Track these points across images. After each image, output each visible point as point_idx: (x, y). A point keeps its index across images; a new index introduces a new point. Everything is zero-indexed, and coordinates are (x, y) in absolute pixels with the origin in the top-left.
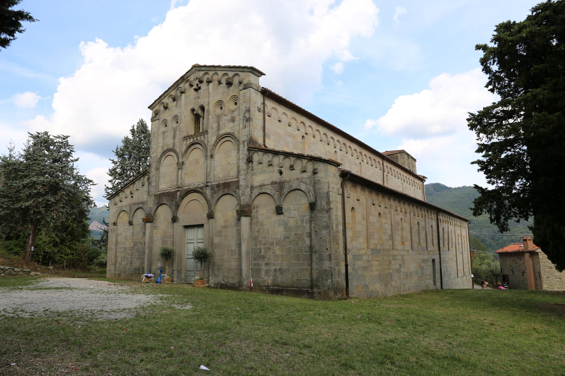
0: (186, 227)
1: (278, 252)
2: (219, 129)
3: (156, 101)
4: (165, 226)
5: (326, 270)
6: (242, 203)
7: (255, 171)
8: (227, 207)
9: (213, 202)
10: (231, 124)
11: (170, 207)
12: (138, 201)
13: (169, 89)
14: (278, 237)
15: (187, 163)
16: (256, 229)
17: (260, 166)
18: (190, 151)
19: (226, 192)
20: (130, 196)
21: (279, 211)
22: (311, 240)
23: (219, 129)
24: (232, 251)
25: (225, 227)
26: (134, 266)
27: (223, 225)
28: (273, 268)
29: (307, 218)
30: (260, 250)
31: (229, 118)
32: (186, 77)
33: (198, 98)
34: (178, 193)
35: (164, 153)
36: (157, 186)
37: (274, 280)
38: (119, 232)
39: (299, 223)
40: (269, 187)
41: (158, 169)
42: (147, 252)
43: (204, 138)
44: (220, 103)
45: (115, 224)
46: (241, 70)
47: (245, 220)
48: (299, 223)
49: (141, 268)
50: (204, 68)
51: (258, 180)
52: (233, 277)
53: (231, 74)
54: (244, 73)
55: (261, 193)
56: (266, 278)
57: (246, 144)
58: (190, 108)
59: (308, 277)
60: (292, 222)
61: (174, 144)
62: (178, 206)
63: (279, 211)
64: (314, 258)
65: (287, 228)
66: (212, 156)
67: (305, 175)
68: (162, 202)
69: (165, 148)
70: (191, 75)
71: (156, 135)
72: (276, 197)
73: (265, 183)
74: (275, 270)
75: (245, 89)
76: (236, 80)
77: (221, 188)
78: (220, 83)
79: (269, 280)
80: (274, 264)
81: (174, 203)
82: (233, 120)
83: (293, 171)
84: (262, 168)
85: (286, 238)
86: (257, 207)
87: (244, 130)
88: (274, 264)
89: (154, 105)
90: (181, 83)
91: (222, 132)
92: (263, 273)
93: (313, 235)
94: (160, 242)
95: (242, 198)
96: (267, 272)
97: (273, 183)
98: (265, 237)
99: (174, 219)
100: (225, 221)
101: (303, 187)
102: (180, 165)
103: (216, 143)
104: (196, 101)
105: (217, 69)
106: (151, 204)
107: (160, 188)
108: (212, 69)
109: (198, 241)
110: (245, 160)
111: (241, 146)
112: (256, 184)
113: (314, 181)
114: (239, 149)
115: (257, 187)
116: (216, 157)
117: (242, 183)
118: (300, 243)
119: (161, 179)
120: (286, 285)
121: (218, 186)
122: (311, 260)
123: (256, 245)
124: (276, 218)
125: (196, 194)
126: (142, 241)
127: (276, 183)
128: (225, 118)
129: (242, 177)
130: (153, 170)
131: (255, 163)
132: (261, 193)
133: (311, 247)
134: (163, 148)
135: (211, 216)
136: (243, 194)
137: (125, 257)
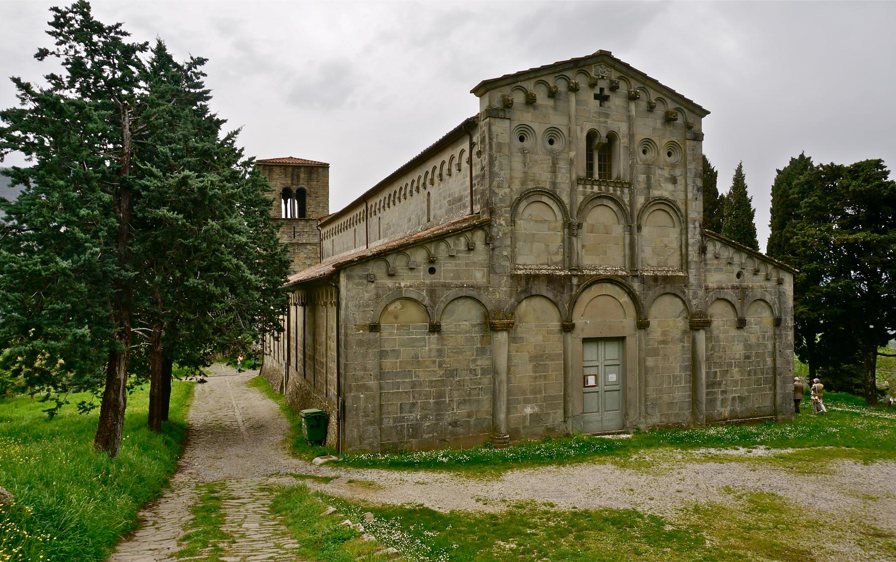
0: (586, 341)
1: (737, 377)
2: (649, 187)
3: (506, 77)
4: (540, 338)
5: (789, 394)
6: (694, 309)
7: (708, 267)
8: (667, 315)
9: (645, 303)
10: (670, 187)
11: (555, 304)
12: (458, 282)
13: (544, 68)
14: (738, 356)
15: (585, 225)
16: (710, 346)
17: (716, 262)
18: (590, 206)
19: (668, 290)
20: (423, 268)
21: (741, 324)
22: (774, 360)
23: (649, 187)
24: (675, 377)
25: (664, 342)
26: (448, 418)
27: (661, 339)
28: (730, 396)
29: (770, 333)
30: (715, 372)
31: (666, 173)
32: (582, 64)
33: (607, 116)
34: (575, 281)
35: (526, 195)
36: (512, 258)
37: (732, 411)
38: (387, 347)
39: (761, 341)
40: (730, 291)
41: (513, 222)
42: (504, 388)
43: (622, 192)
44: (647, 145)
45: (374, 328)
46: (690, 106)
47: (701, 336)
48: (761, 340)
49: (472, 420)
50: (624, 69)
51: (714, 279)
52: (677, 415)
53: (671, 106)
54: (692, 115)
55: (718, 299)
56: (722, 410)
57: (697, 224)
58: (588, 127)
59: (768, 403)
60: (753, 340)
61: (554, 184)
62: (573, 303)
63: (741, 324)
64: (778, 383)
65: (748, 347)
66: (639, 228)
67: (768, 284)
68: (534, 292)
69: (531, 185)
70: (591, 65)
71: (506, 150)
72: (738, 306)
73: (724, 285)
74: (734, 399)
75: (694, 140)
76: (680, 121)
77: (659, 283)
78: (651, 108)
79: (726, 412)
80: (732, 391)
81: (566, 296)
82: (674, 180)
83: (755, 278)
84: (718, 265)
85: (747, 357)
86: (711, 317)
87: (694, 203)
88: (732, 391)
89: (499, 83)
90: (571, 69)
91: (656, 193)
92: (719, 403)
93: (778, 355)
94: (530, 367)
95: (694, 302)
96: (723, 401)
97: (733, 287)
98: (721, 357)
99: (567, 327)
100: (664, 333)
101: (768, 298)
102: (572, 228)
103: (645, 207)
104: (602, 119)
105: (648, 82)
106: (501, 293)
107: (518, 262)
108: (639, 78)
109: (607, 363)
110: (696, 248)
111: (691, 226)
112: (710, 285)
113: (780, 292)
114: (687, 228)
115: (714, 289)
116: (645, 230)
117: (692, 279)
118: (761, 364)
119: (520, 244)
120: (748, 414)
121: (655, 278)
122: (775, 384)
123: (710, 368)
124: (734, 332)
125: (609, 285)
126: (472, 366)
127: (737, 288)
128: (659, 172)
129: (692, 272)
130: (501, 221)
131: (709, 255)
132: (718, 299)
133: (774, 368)
134: (524, 182)
135: (643, 325)
136: (695, 295)
137: (414, 405)
